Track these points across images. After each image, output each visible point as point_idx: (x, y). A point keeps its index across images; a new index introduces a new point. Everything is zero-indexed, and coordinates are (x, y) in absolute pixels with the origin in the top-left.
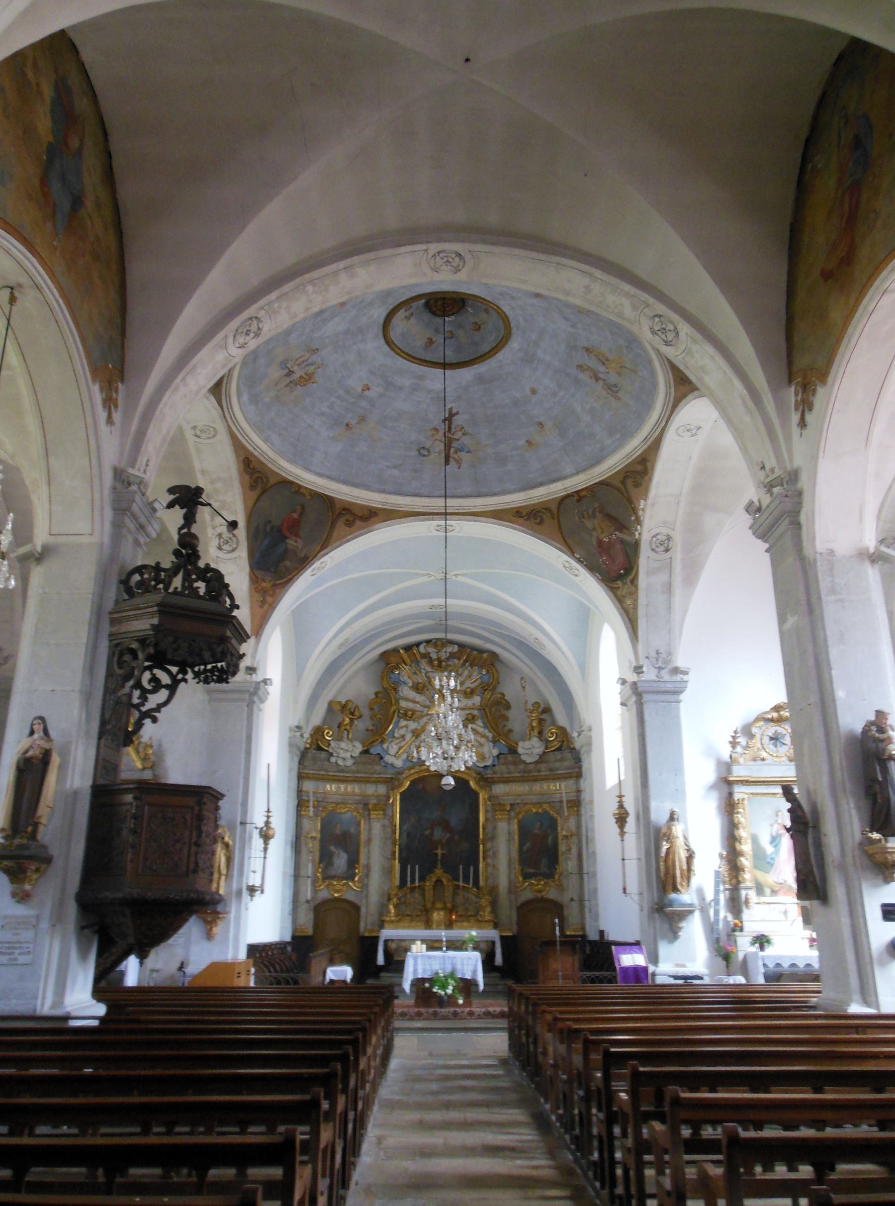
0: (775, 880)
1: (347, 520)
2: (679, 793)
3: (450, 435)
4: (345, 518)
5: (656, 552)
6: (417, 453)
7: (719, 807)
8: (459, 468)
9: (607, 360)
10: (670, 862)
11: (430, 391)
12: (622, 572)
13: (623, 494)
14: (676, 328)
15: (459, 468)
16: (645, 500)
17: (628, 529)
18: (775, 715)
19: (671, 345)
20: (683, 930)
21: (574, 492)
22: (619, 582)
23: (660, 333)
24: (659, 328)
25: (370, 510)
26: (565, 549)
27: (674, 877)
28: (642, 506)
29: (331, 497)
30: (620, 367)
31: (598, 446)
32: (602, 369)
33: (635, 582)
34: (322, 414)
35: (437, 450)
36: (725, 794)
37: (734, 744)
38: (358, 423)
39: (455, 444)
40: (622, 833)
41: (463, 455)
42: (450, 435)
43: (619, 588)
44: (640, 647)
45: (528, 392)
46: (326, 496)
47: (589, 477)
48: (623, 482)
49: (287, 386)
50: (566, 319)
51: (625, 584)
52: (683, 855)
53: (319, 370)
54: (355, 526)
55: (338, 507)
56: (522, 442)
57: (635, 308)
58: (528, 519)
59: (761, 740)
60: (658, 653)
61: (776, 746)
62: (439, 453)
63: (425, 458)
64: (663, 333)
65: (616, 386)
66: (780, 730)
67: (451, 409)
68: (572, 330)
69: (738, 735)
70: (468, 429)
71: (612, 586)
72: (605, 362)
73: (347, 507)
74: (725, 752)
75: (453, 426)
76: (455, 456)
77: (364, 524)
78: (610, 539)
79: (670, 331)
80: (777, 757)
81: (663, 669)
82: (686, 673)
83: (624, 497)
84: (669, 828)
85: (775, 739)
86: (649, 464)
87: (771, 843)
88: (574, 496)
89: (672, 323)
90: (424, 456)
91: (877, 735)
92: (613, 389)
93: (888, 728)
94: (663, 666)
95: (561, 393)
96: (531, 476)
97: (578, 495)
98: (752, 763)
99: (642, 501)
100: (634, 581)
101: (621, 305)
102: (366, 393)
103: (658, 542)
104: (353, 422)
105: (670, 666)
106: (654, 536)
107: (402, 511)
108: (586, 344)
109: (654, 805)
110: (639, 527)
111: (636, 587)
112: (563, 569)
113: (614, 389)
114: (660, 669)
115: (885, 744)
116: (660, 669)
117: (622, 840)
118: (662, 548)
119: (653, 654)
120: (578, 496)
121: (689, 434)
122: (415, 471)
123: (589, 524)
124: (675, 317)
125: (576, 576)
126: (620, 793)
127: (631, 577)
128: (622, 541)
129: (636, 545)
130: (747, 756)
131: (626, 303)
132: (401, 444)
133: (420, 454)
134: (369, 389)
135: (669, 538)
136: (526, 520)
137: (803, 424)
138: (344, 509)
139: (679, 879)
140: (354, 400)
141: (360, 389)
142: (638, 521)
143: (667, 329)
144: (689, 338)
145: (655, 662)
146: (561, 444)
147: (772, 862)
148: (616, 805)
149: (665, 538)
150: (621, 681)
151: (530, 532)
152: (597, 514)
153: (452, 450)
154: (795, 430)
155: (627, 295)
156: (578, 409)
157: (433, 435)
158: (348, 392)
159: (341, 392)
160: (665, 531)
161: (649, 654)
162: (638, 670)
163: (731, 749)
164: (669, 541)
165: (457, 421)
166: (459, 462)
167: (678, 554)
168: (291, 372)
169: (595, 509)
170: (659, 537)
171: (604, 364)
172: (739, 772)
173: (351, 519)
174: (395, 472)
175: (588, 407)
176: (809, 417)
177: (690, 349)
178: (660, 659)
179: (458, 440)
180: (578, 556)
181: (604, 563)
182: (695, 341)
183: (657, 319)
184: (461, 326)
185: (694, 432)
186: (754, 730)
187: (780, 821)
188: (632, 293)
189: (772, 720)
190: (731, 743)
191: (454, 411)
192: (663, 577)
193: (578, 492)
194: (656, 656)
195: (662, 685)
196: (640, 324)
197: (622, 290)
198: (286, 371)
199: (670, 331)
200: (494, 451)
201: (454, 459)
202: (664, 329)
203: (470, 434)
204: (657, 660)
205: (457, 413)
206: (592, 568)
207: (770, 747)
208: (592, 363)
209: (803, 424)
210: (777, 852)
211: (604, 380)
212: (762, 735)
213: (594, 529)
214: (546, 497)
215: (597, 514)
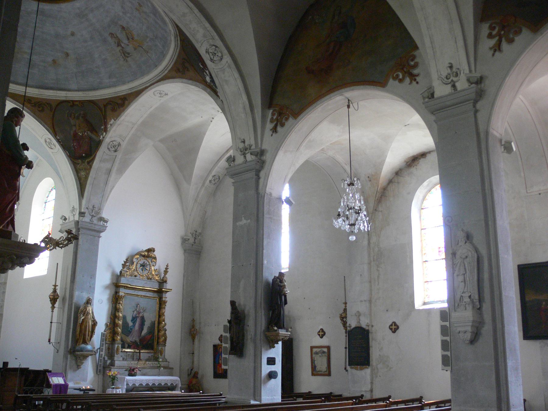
0: (131, 340)
2: (92, 289)
5: (109, 150)
7: (108, 299)
9: (133, 39)
10: (83, 327)
12: (84, 155)
13: (101, 111)
14: (222, 56)
16: (115, 120)
17: (96, 132)
18: (146, 253)
19: (213, 62)
20: (84, 364)
21: (71, 101)
22: (79, 160)
23: (211, 54)
24: (212, 51)
26: (51, 131)
27: (85, 335)
28: (111, 122)
30: (138, 46)
32: (126, 41)
33: (91, 164)
36: (113, 292)
37: (124, 266)
40: (53, 307)
43: (79, 164)
44: (84, 202)
45: (69, 33)
47: (85, 95)
48: (105, 106)
51: (83, 162)
52: (91, 323)
56: (50, 59)
57: (204, 36)
58: (35, 106)
59: (136, 265)
60: (93, 207)
61: (142, 271)
64: (213, 55)
65: (129, 54)
66: (146, 262)
68: (121, 14)
69: (127, 261)
71: (76, 162)
74: (118, 269)
78: (83, 134)
79: (217, 56)
80: (142, 275)
81: (94, 216)
82: (106, 222)
83: (102, 114)
84: (85, 308)
85: (143, 265)
86: (126, 102)
87: (132, 321)
88: (70, 102)
89: (222, 53)
91: (280, 284)
92: (126, 55)
93: (284, 281)
94: (95, 215)
97: (73, 104)
98: (130, 277)
99: (113, 120)
100: (90, 163)
103: (113, 145)
105: (98, 216)
106: (112, 141)
108: (125, 26)
109: (76, 293)
110: (104, 134)
111: (91, 167)
112: (43, 141)
113: (126, 55)
114: (93, 216)
115: (282, 288)
116: (93, 216)
117: (53, 311)
118: (114, 149)
119: (91, 207)
120: (72, 104)
121: (160, 95)
123: (72, 122)
124: (225, 51)
125: (51, 148)
126: (56, 283)
127: (89, 160)
128: (90, 138)
129: (99, 144)
130: (128, 273)
135: (119, 145)
136: (32, 106)
137: (274, 130)
139: (87, 336)
142: (106, 130)
143: (217, 54)
144: (227, 64)
145: (91, 211)
147: (131, 331)
148: (52, 291)
149: (117, 144)
150: (64, 218)
151: (32, 114)
152: (80, 118)
154: (268, 132)
155: (205, 28)
156: (96, 56)
160: (119, 140)
161: (88, 206)
162: (82, 214)
163: (122, 268)
164: (119, 146)
167: (119, 155)
170: (114, 142)
171: (128, 39)
172: (123, 281)
175: (103, 57)
176: (279, 128)
177: (224, 70)
178: (94, 211)
180: (58, 138)
181: (74, 147)
182: (229, 67)
183: (214, 47)
185: (162, 95)
186: (134, 260)
187: (138, 310)
188: (208, 29)
189: (144, 256)
190: (123, 265)
192: (108, 165)
193: (73, 101)
194: (92, 208)
195: (93, 226)
197: (204, 25)
199: (217, 56)
202: (215, 54)
204: (92, 211)
206: (65, 147)
207: (140, 270)
208: (122, 36)
209: (274, 130)
210: (134, 325)
211: (123, 48)
212: (137, 263)
213: (75, 125)
215: (80, 118)
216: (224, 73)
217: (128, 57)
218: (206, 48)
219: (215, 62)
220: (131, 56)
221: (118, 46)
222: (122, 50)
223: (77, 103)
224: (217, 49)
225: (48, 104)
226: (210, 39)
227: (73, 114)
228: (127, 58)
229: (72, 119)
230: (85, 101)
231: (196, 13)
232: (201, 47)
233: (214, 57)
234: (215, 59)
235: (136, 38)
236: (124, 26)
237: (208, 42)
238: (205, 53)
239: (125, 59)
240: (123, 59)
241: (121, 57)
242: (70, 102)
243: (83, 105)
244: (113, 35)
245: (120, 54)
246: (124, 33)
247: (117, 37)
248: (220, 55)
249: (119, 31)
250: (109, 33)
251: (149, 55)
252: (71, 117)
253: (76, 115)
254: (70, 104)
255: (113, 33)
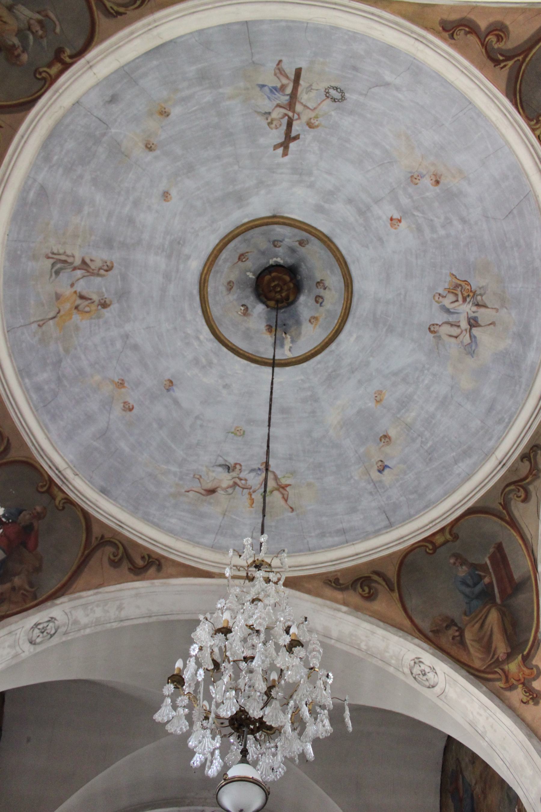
1: (499, 38)
3: (290, 114)
4: (501, 45)
6: (347, 95)
8: (280, 61)
9: (76, 308)
11: (311, 186)
15: (280, 61)
19: (32, 627)
24: (49, 627)
25: (452, 37)
29: (507, 96)
31: (56, 158)
34: (463, 221)
35: (313, 94)
38: (421, 176)
39: (285, 99)
41: (272, 81)
42: (290, 114)
45: (174, 193)
46: (515, 105)
49: (485, 306)
50: (136, 347)
53: (440, 290)
54: (492, 20)
55: (506, 71)
56: (176, 111)
57: (76, 622)
62: (310, 89)
63: (333, 84)
64: (43, 628)
65: (57, 273)
67: (285, 154)
70: (264, 123)
72: (79, 301)
73: (491, 64)
75: (284, 127)
76: (285, 81)
77: (472, 17)
79: (39, 636)
88: (71, 57)
90: (336, 89)
95: (126, 210)
96: (155, 63)
101: (87, 615)
102: (396, 216)
104: (427, 182)
107: (393, 13)
113: (59, 266)
122: (355, 68)
131: (84, 620)
132: (369, 116)
133: (342, 92)
134: (391, 219)
138: (496, 62)
140: (416, 213)
141: (403, 225)
143: (41, 635)
146: (113, 130)
152: (16, 41)
153: (289, 90)
155: (85, 627)
156: (99, 198)
157: (316, 117)
158: (419, 229)
159: (428, 234)
165: (278, 135)
166: (279, 70)
168: (473, 323)
169: (25, 50)
171: (82, 297)
173: (492, 38)
174: (388, 77)
175: (86, 209)
179: (278, 106)
182: (16, 655)
184: (263, 253)
191: (280, 151)
193: (66, 66)
196: (66, 614)
198: (475, 331)
200: (221, 90)
201: (287, 77)
202: (43, 633)
203: (258, 113)
205: (276, 147)
211: (75, 269)
214: (121, 39)
215: (16, 41)
216: (9, 646)
217: (53, 265)
218: (57, 618)
219: (32, 630)
220: (51, 275)
221: (84, 262)
222: (72, 263)
223: (53, 71)
224: (49, 636)
225: (121, 14)
226: (67, 628)
227: (40, 33)
228: (52, 261)
229: (31, 18)
230: (43, 90)
231: (113, 624)
232: (63, 611)
233: (39, 629)
234: (36, 631)
235: (76, 317)
236: (104, 311)
237: (64, 625)
238: (51, 615)
239: (54, 256)
240: (56, 251)
241: (61, 251)
242: (71, 57)
243: (38, 76)
244: (105, 268)
245: (69, 252)
246: (95, 297)
247: (98, 275)
248: (38, 640)
249: (104, 290)
250: (115, 265)
251: (34, 326)
252: (40, 22)
253: (31, 37)
254: (68, 52)
255: (110, 273)
